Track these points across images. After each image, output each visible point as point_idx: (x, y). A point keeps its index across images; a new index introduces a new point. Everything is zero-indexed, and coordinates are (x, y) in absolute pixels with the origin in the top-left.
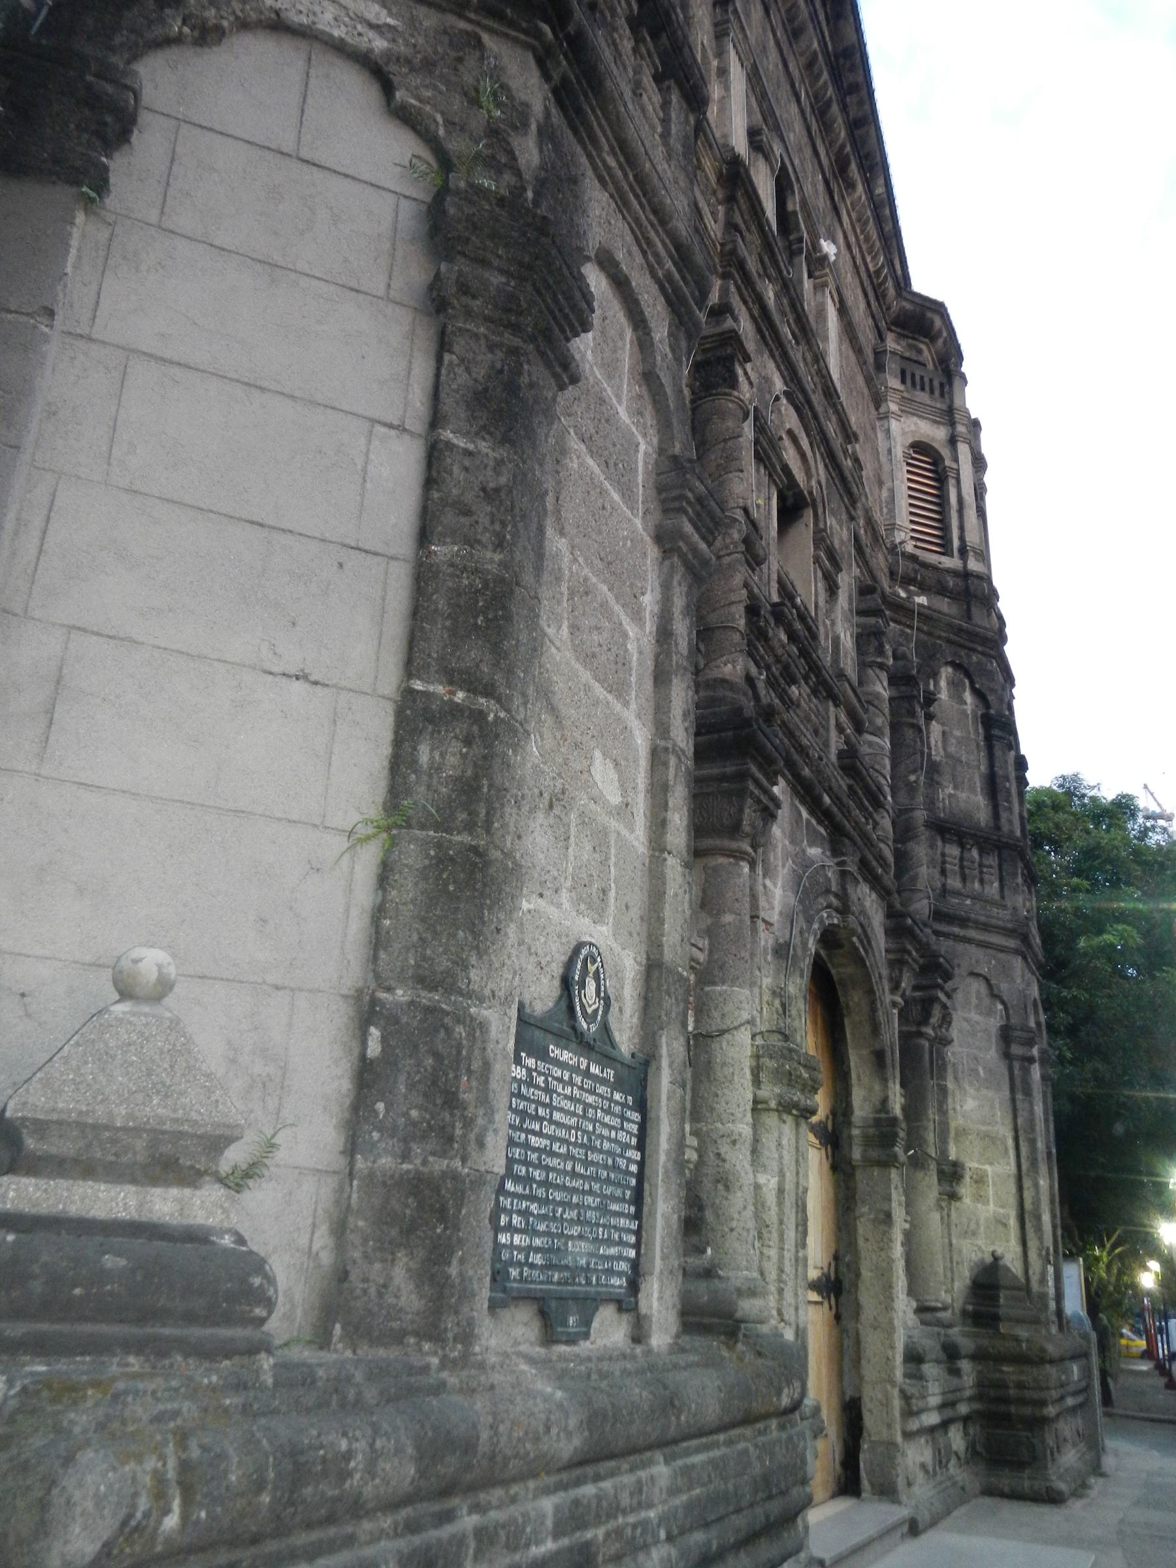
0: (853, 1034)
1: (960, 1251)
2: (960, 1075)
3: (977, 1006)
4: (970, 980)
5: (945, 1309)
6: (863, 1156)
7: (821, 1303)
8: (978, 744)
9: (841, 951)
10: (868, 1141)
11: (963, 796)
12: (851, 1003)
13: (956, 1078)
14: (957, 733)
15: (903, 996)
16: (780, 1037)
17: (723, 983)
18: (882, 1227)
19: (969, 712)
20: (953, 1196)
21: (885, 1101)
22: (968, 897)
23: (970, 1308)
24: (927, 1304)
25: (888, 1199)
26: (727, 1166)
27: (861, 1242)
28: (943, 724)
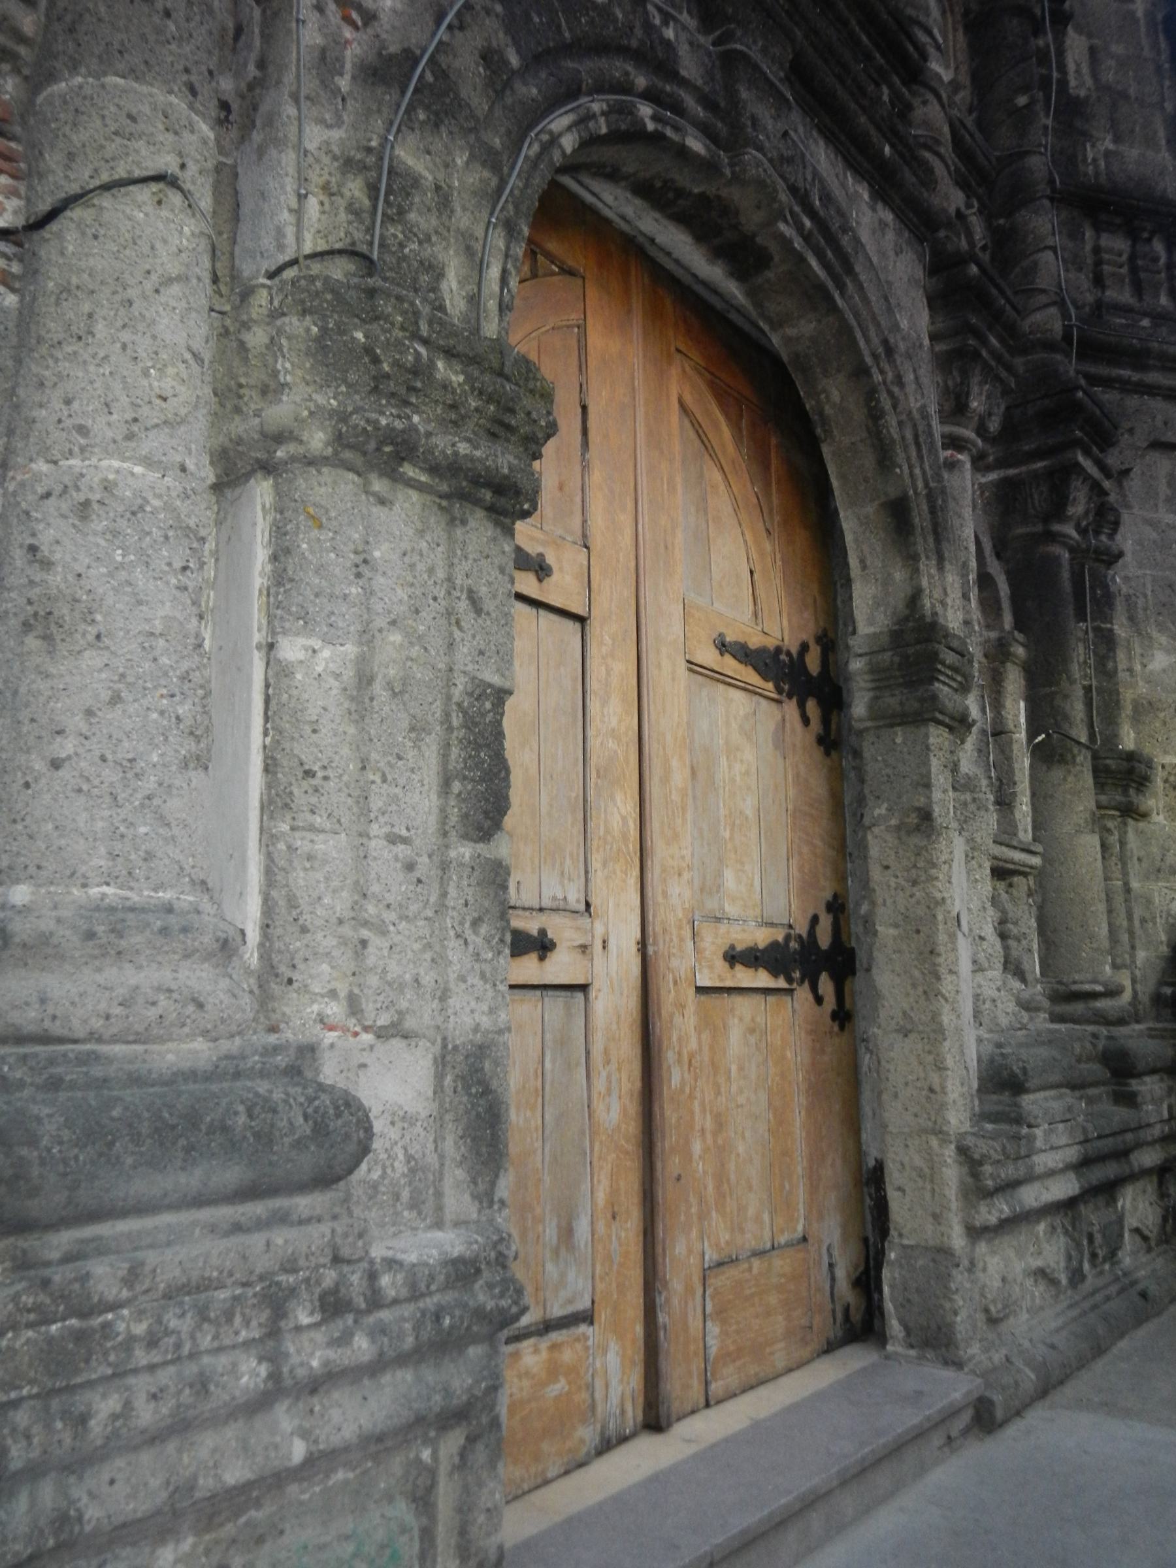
0: (843, 477)
1: (1149, 901)
2: (1141, 614)
3: (1168, 500)
4: (1154, 456)
5: (1112, 992)
6: (870, 707)
7: (790, 992)
8: (1159, 69)
9: (770, 274)
10: (881, 678)
11: (1133, 153)
12: (828, 410)
13: (1131, 619)
14: (1117, 49)
15: (981, 430)
16: (352, 267)
17: (74, 68)
18: (916, 840)
19: (1140, 14)
20: (1130, 812)
21: (914, 599)
22: (1145, 314)
23: (1168, 991)
24: (1075, 987)
25: (926, 785)
26: (56, 579)
27: (876, 873)
28: (1090, 36)
